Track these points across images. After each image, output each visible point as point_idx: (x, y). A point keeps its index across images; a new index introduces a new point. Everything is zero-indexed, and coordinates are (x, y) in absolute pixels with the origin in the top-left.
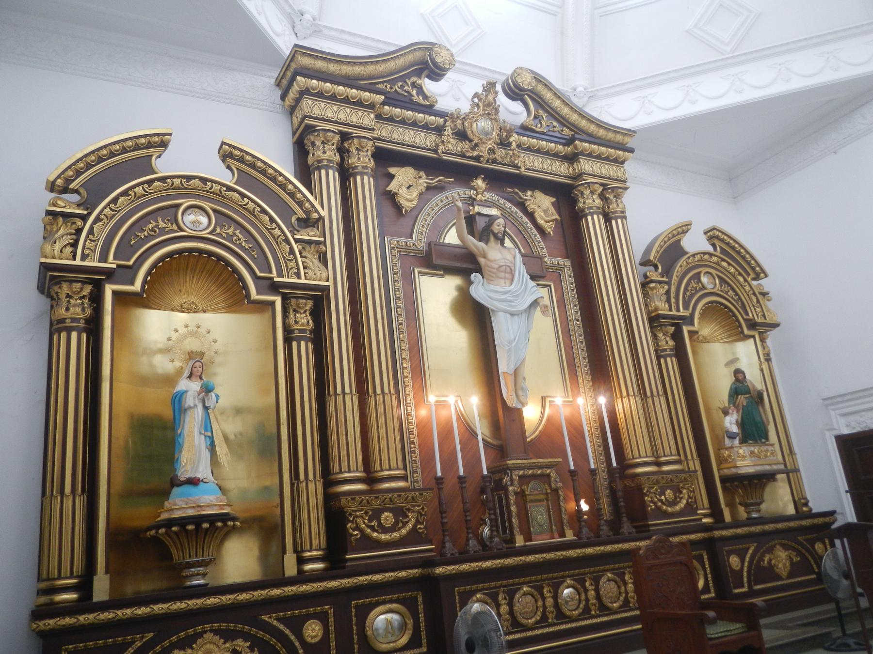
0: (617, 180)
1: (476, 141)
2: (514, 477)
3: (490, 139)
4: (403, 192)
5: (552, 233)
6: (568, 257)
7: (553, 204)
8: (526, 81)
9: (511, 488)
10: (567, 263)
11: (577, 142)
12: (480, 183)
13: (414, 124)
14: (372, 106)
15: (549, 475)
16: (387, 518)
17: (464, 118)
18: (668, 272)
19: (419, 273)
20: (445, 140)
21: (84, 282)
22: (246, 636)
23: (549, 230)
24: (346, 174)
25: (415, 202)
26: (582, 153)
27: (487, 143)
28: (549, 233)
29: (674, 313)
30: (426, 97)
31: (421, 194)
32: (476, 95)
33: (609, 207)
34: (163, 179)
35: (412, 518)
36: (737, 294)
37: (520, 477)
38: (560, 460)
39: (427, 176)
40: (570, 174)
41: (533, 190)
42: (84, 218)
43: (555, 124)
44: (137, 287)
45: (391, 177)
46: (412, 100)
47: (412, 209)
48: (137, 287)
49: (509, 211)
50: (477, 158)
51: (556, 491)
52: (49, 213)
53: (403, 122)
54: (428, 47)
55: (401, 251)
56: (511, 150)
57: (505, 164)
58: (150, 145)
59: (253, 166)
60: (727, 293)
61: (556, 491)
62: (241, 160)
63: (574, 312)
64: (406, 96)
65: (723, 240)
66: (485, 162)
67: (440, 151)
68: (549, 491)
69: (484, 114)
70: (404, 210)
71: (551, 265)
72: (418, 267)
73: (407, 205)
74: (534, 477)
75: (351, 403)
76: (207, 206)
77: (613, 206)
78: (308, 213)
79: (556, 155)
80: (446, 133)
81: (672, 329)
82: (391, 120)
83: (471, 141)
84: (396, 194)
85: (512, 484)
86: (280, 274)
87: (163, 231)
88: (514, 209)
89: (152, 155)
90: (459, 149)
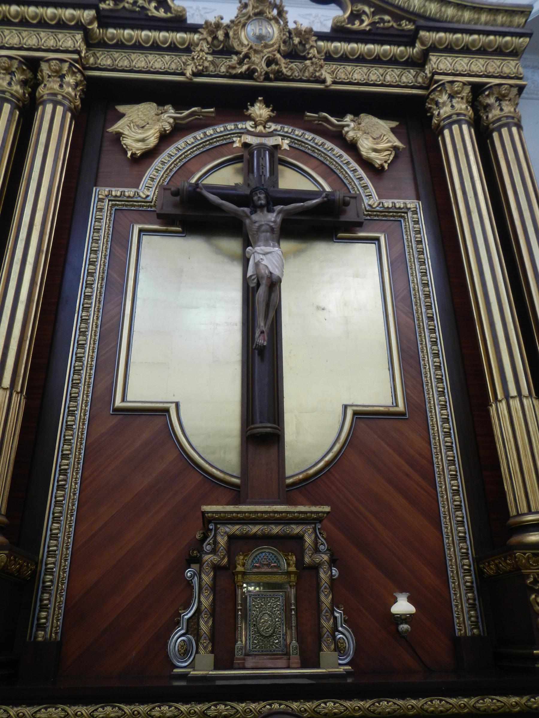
1: (245, 50)
2: (219, 539)
3: (266, 46)
5: (386, 166)
6: (418, 198)
7: (393, 130)
9: (207, 558)
10: (412, 204)
11: (422, 33)
14: (79, 26)
15: (300, 538)
17: (228, 26)
20: (195, 57)
23: (379, 162)
25: (152, 141)
26: (434, 48)
27: (262, 52)
28: (382, 166)
33: (487, 117)
37: (232, 538)
38: (327, 509)
39: (176, 110)
40: (419, 83)
41: (356, 114)
43: (387, 18)
45: (122, 116)
46: (147, 15)
49: (313, 145)
50: (250, 74)
51: (315, 568)
53: (138, 47)
55: (115, 205)
56: (311, 59)
57: (301, 81)
61: (315, 568)
64: (139, 12)
66: (262, 78)
67: (188, 72)
68: (293, 569)
69: (256, 14)
70: (129, 154)
71: (381, 209)
77: (494, 114)
79: (393, 61)
82: (120, 45)
83: (237, 53)
85: (214, 551)
90: (223, 69)
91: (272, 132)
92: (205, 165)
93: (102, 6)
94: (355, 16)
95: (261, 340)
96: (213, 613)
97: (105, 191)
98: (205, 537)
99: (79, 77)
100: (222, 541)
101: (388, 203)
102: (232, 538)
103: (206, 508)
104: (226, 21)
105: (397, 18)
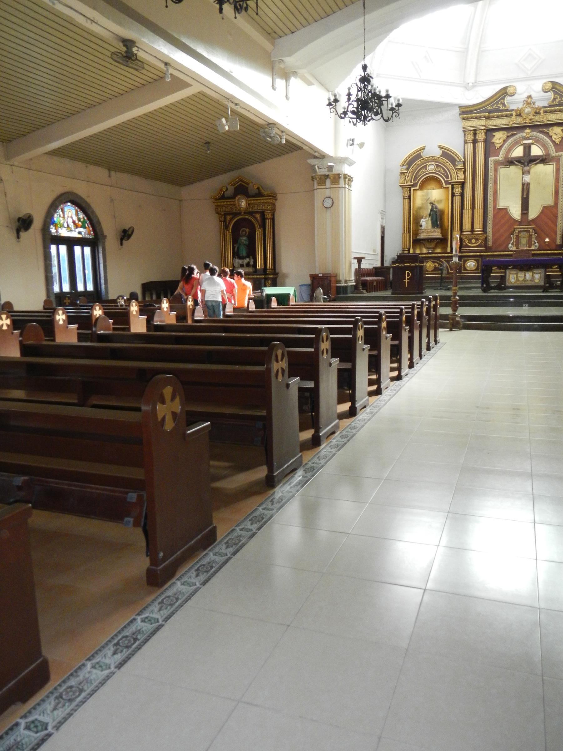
4: (497, 141)
9: (515, 234)
12: (528, 131)
13: (502, 116)
14: (485, 117)
15: (530, 231)
16: (473, 241)
19: (501, 168)
21: (407, 188)
22: (437, 263)
24: (475, 142)
32: (524, 101)
34: (423, 159)
35: (480, 241)
42: (407, 173)
44: (417, 188)
48: (417, 188)
50: (526, 123)
51: (532, 235)
54: (505, 89)
58: (420, 150)
59: (445, 149)
61: (532, 235)
72: (499, 165)
73: (498, 146)
74: (524, 231)
75: (470, 211)
76: (434, 163)
78: (460, 160)
80: (513, 117)
84: (494, 143)
86: (451, 180)
87: (424, 172)
89: (421, 153)
91: (531, 136)
92: (515, 146)
93: (489, 108)
94: (554, 99)
95: (525, 196)
96: (516, 242)
97: (493, 158)
98: (514, 231)
99: (485, 131)
100: (517, 232)
101: (558, 154)
102: (519, 231)
103: (515, 227)
104: (520, 108)
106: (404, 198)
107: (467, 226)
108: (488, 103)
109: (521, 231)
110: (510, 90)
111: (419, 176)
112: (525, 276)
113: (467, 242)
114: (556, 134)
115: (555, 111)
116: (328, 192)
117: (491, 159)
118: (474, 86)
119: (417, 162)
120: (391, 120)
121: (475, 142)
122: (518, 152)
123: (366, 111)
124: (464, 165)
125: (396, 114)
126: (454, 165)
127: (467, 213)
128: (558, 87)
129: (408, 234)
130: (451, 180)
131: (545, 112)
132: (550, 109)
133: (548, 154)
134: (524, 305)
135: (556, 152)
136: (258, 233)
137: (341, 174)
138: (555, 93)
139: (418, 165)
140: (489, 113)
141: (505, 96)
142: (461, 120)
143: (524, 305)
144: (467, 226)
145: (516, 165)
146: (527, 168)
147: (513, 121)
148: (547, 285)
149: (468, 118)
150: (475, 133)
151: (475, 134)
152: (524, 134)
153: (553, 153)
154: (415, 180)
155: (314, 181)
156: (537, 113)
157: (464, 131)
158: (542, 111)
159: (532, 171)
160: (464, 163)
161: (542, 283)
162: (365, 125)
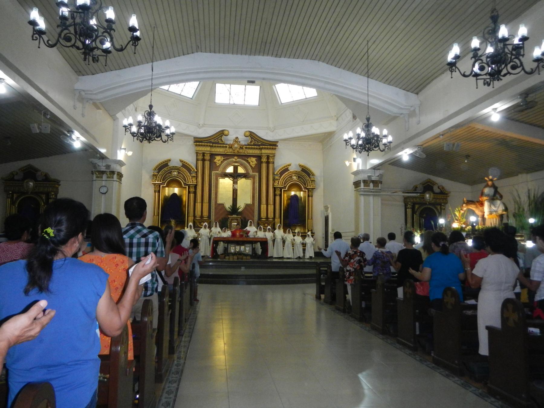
0: (272, 154)
7: (256, 160)
8: (248, 134)
12: (236, 158)
13: (220, 147)
14: (210, 146)
18: (280, 177)
24: (204, 160)
26: (262, 148)
29: (279, 186)
30: (222, 141)
31: (222, 162)
32: (234, 140)
36: (303, 180)
37: (231, 219)
42: (158, 175)
44: (165, 186)
47: (219, 165)
48: (165, 186)
52: (153, 175)
54: (223, 131)
58: (167, 161)
59: (184, 162)
60: (300, 180)
62: (183, 162)
63: (257, 185)
65: (302, 166)
73: (218, 164)
74: (235, 219)
76: (176, 171)
77: (270, 160)
78: (194, 170)
79: (257, 148)
81: (280, 190)
87: (169, 176)
88: (245, 162)
93: (213, 141)
94: (251, 142)
98: (228, 219)
102: (231, 219)
105: (258, 142)
106: (155, 192)
107: (198, 213)
108: (212, 137)
109: (234, 219)
110: (226, 133)
111: (166, 178)
112: (240, 248)
113: (198, 224)
114: (252, 162)
115: (252, 148)
116: (104, 183)
117: (213, 172)
118: (203, 126)
119: (165, 169)
120: (167, 142)
121: (204, 160)
122: (230, 170)
123: (151, 134)
124: (197, 174)
125: (170, 138)
126: (190, 174)
127: (199, 206)
128: (253, 135)
129: (157, 217)
130: (188, 182)
131: (246, 148)
132: (248, 146)
133: (249, 174)
134: (242, 267)
135: (253, 172)
136: (42, 209)
137: (115, 172)
138: (252, 138)
139: (165, 170)
140: (213, 143)
141: (222, 136)
142: (194, 145)
143: (242, 267)
144: (198, 213)
145: (229, 178)
146: (236, 180)
147: (227, 151)
148: (254, 255)
149: (199, 145)
150: (204, 154)
151: (204, 155)
152: (234, 160)
153: (251, 173)
154: (163, 180)
155: (93, 174)
156: (242, 148)
157: (197, 153)
158: (244, 147)
159: (239, 182)
160: (196, 172)
161: (251, 253)
162: (149, 143)
